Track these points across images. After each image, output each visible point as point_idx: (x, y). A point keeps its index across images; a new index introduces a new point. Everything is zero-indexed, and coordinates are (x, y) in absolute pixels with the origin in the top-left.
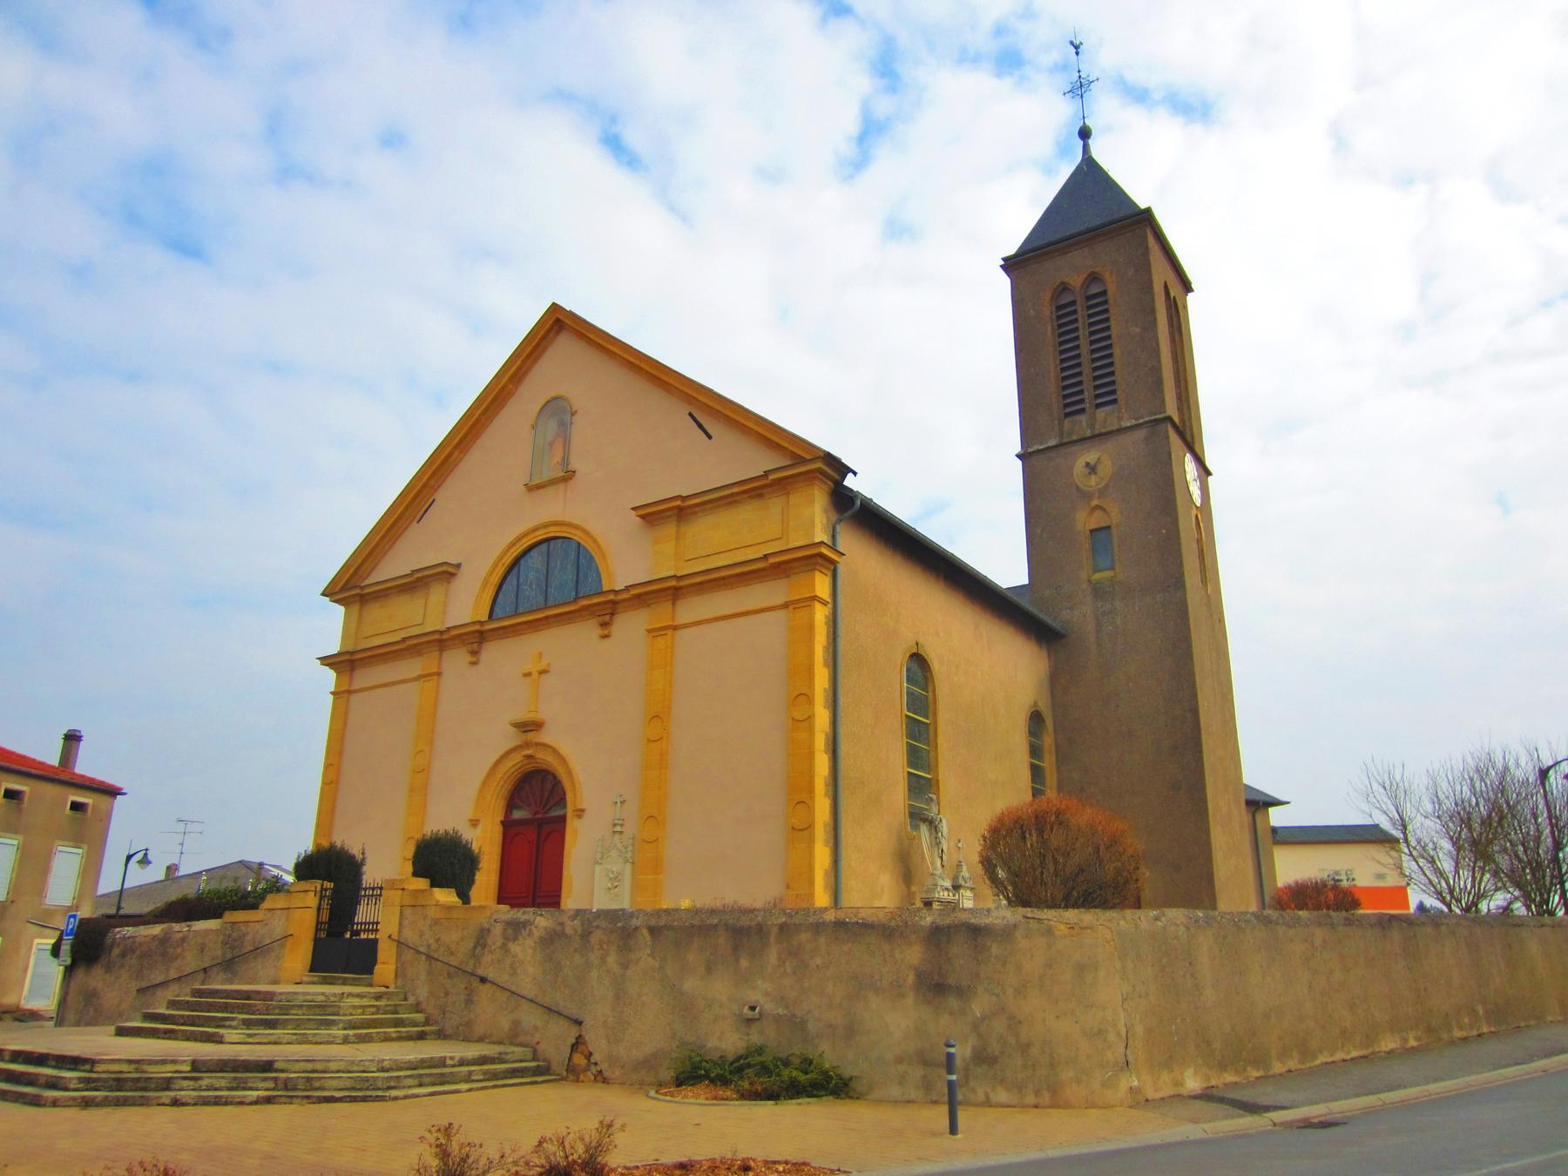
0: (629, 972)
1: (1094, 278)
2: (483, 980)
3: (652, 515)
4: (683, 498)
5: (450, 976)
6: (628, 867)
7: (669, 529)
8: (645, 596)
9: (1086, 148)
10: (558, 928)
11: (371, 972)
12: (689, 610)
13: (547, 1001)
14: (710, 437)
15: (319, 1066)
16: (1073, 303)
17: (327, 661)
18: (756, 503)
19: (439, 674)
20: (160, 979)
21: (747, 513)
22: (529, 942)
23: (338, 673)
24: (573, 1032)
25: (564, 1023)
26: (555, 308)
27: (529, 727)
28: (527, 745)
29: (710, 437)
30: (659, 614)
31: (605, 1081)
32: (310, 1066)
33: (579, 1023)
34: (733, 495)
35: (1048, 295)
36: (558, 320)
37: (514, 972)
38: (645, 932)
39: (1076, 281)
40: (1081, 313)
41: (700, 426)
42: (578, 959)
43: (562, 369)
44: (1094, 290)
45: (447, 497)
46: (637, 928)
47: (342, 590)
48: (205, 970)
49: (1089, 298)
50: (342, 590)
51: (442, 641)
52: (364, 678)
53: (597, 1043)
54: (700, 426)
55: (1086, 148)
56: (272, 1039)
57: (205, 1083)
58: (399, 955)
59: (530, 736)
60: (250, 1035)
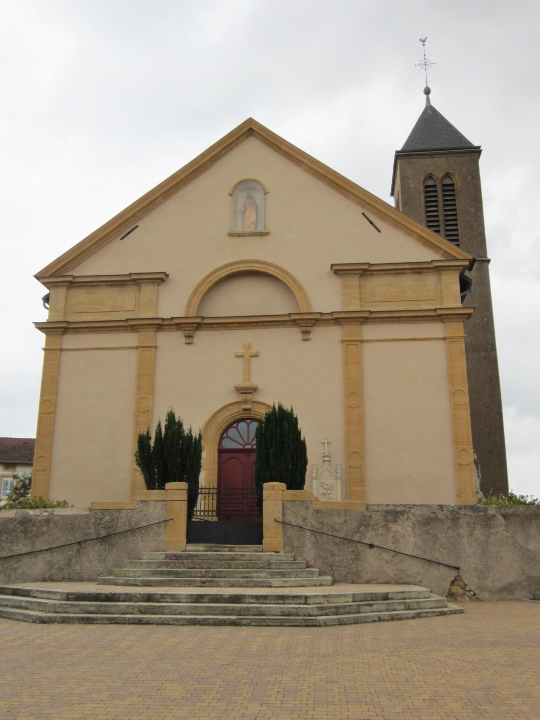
0: (490, 540)
1: (447, 175)
2: (371, 546)
3: (339, 271)
4: (369, 264)
5: (337, 544)
6: (339, 482)
7: (354, 281)
8: (337, 320)
9: (428, 100)
10: (432, 515)
11: (261, 543)
12: (370, 331)
13: (427, 557)
14: (379, 231)
15: (407, 596)
16: (435, 186)
17: (41, 327)
18: (416, 276)
19: (156, 347)
20: (24, 550)
21: (408, 281)
22: (408, 523)
23: (47, 335)
24: (453, 574)
25: (446, 570)
26: (250, 118)
27: (243, 391)
28: (245, 402)
29: (379, 231)
30: (352, 330)
31: (478, 599)
32: (403, 596)
33: (458, 568)
34: (405, 269)
35: (422, 178)
36: (251, 129)
37: (396, 541)
38: (500, 517)
39: (439, 175)
40: (440, 193)
41: (371, 223)
42: (451, 532)
43: (250, 159)
44: (447, 181)
45: (147, 226)
46: (494, 516)
47: (51, 276)
48: (80, 543)
49: (444, 185)
50: (51, 276)
51: (161, 325)
52: (70, 341)
53: (470, 579)
54: (371, 223)
55: (428, 100)
56: (297, 584)
57: (375, 607)
58: (285, 532)
59: (249, 396)
60: (285, 582)
